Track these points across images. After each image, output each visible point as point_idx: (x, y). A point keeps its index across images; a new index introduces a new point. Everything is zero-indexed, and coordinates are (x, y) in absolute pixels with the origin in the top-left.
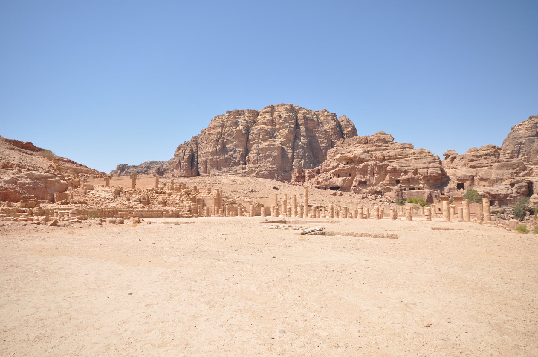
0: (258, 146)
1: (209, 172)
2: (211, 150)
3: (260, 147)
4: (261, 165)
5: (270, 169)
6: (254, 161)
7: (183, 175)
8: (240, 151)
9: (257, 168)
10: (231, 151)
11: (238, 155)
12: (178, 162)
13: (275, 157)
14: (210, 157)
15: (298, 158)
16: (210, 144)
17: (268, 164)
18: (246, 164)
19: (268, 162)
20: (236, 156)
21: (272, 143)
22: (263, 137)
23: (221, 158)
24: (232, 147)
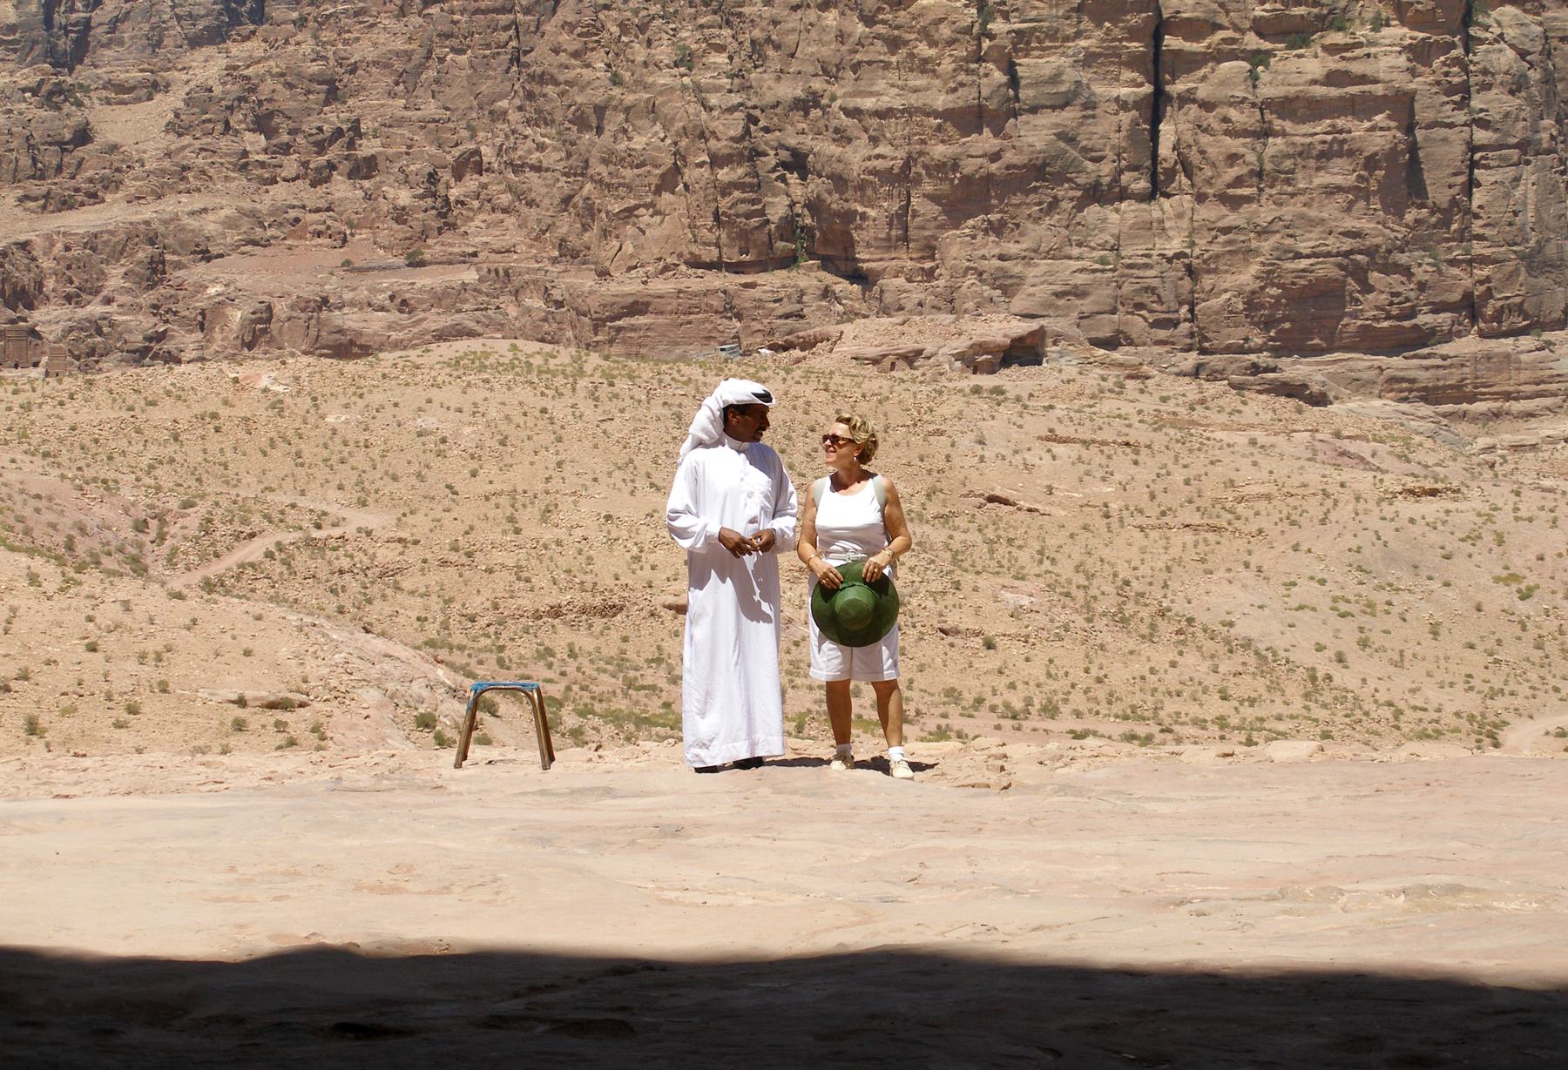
0: (1254, 77)
1: (930, 250)
2: (941, 101)
3: (1266, 91)
4: (1289, 211)
5: (1348, 244)
6: (1238, 182)
7: (711, 254)
8: (1123, 105)
9: (1263, 232)
10: (1064, 103)
11: (1110, 129)
12: (668, 161)
13: (1371, 163)
14: (939, 151)
15: (1506, 162)
16: (924, 50)
17: (1330, 210)
18: (1157, 189)
19: (1331, 191)
20: (1096, 142)
21: (1357, 68)
22: (1278, 18)
23: (1010, 157)
24: (1071, 75)
